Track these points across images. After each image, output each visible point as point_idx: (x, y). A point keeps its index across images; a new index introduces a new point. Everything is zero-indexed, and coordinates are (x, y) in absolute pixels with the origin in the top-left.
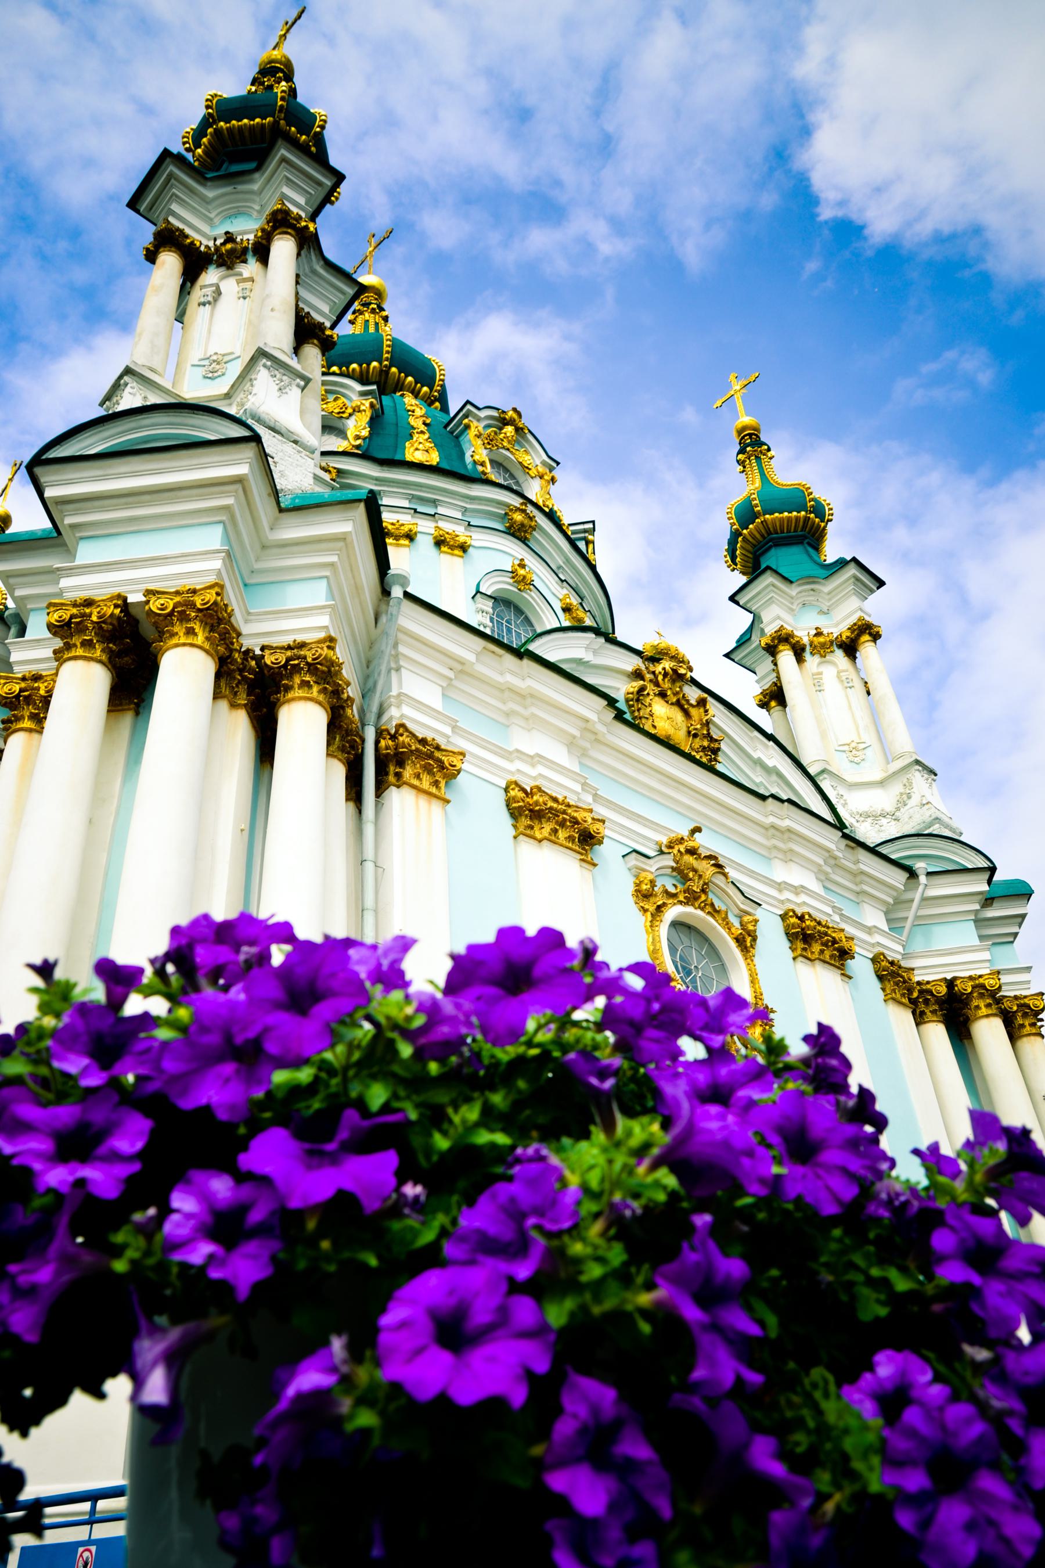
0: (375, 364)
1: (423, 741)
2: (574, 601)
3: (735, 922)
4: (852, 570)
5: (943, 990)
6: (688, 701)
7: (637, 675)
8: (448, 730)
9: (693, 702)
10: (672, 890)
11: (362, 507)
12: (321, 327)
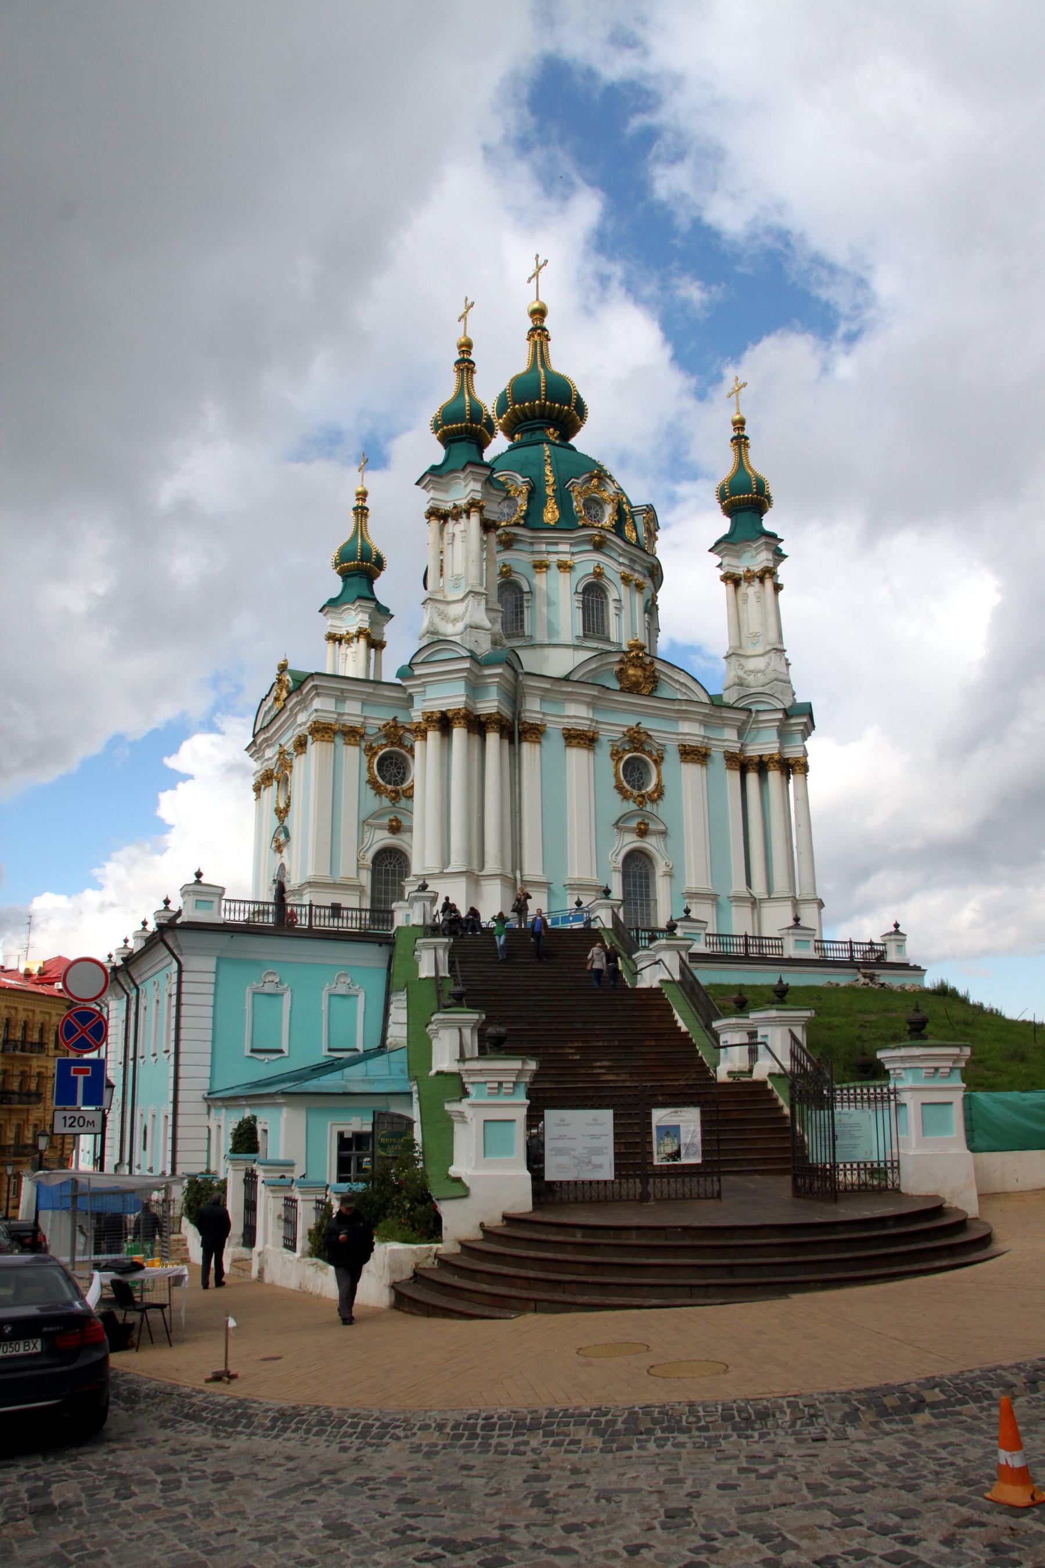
2: (628, 571)
3: (655, 753)
4: (763, 540)
5: (756, 760)
7: (621, 661)
8: (541, 716)
10: (627, 748)
12: (494, 522)
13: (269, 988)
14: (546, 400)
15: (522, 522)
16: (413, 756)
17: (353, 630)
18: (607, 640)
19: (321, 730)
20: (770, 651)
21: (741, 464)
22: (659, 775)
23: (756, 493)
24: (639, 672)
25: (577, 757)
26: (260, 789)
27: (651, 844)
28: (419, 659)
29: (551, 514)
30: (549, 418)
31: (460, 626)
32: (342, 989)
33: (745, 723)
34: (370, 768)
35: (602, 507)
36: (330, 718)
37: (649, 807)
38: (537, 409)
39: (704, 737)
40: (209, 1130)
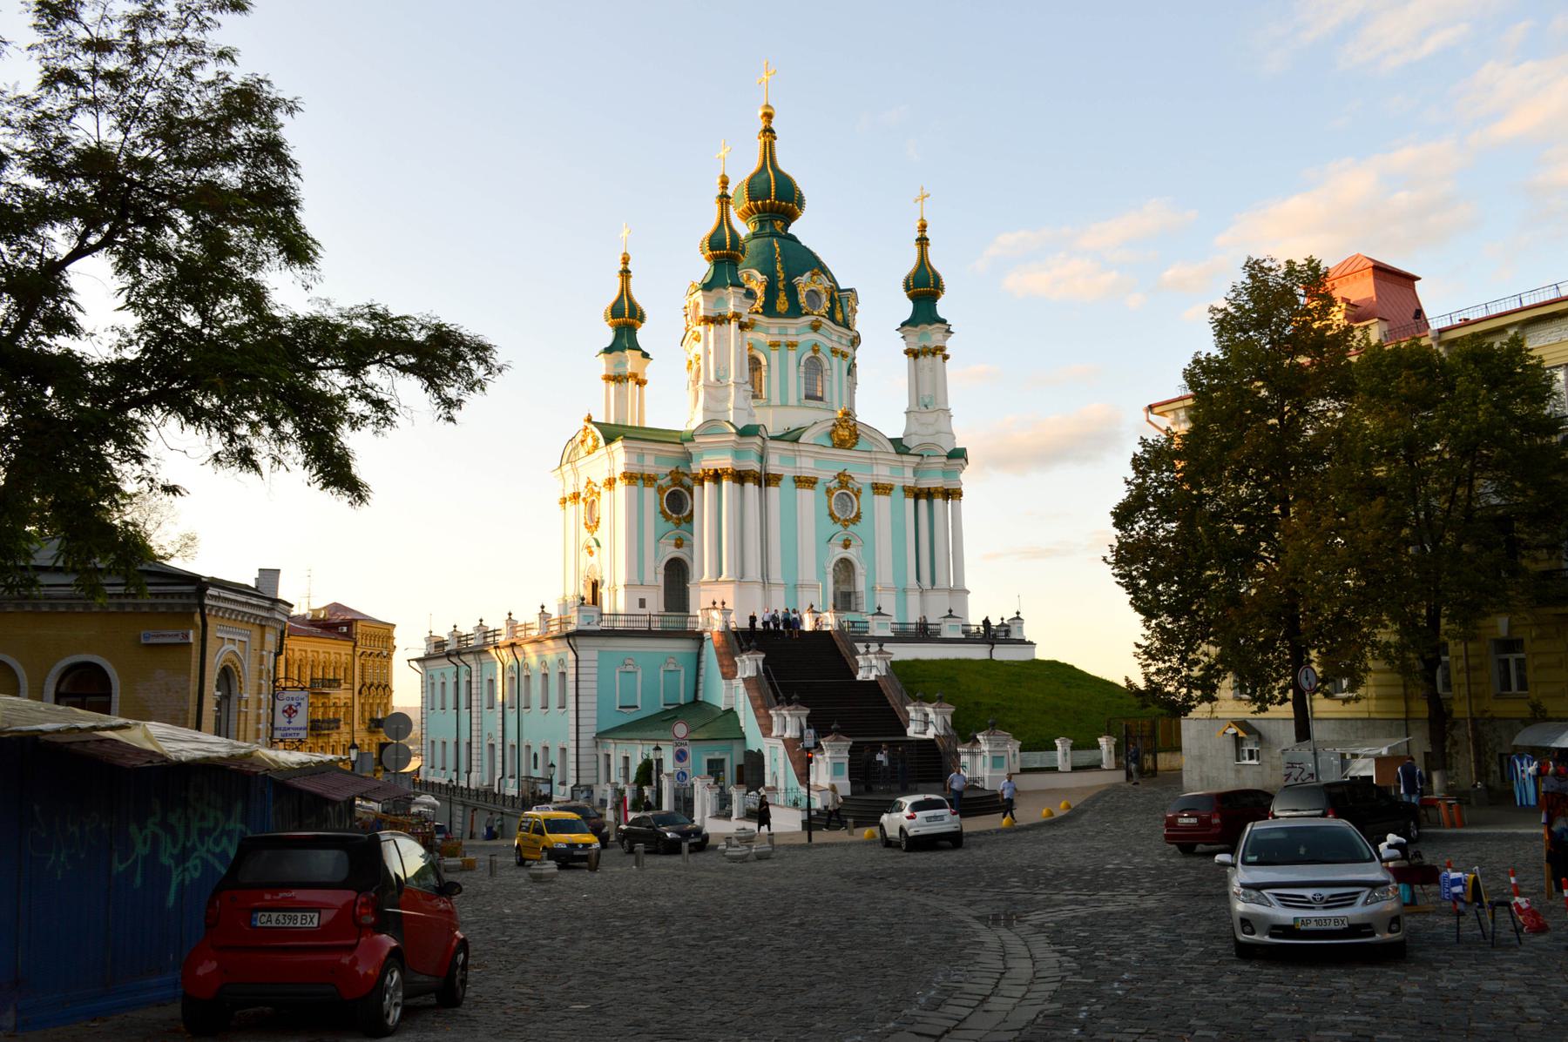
13: (630, 668)
16: (692, 494)
19: (630, 477)
21: (923, 261)
25: (807, 496)
27: (851, 554)
29: (782, 304)
32: (672, 667)
36: (636, 470)
37: (852, 528)
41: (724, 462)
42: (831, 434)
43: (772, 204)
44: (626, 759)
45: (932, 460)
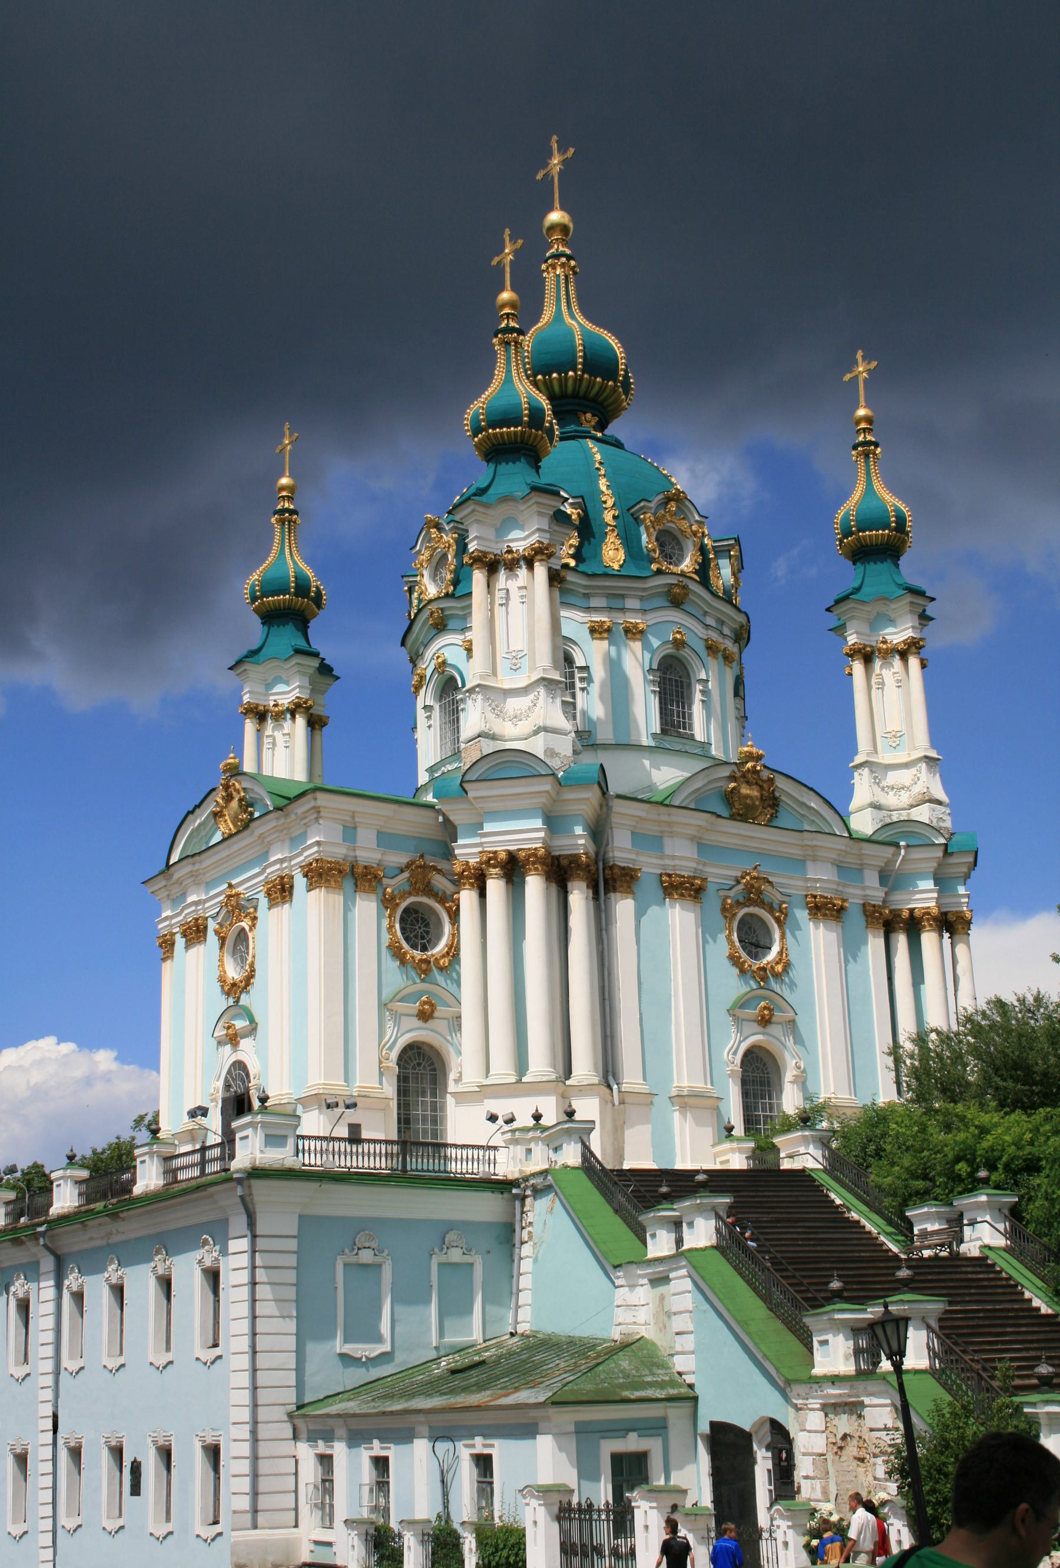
0: (571, 373)
1: (624, 868)
2: (714, 636)
3: (776, 906)
4: (909, 598)
5: (905, 914)
6: (762, 781)
7: (732, 778)
9: (765, 778)
10: (741, 900)
11: (596, 786)
13: (366, 1256)
14: (584, 371)
15: (572, 563)
17: (285, 701)
18: (692, 738)
20: (919, 760)
22: (783, 937)
23: (896, 529)
24: (755, 793)
26: (173, 944)
28: (471, 776)
30: (585, 398)
31: (525, 727)
32: (456, 1255)
33: (890, 862)
34: (391, 927)
35: (679, 543)
36: (338, 852)
37: (774, 985)
38: (570, 383)
39: (838, 884)
40: (297, 1462)
41: (525, 833)
42: (729, 797)
43: (578, 380)
44: (381, 1464)
45: (917, 854)
